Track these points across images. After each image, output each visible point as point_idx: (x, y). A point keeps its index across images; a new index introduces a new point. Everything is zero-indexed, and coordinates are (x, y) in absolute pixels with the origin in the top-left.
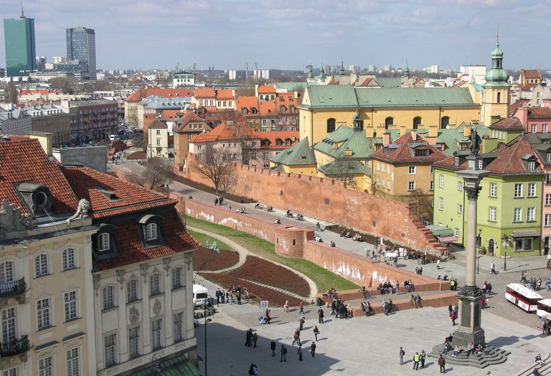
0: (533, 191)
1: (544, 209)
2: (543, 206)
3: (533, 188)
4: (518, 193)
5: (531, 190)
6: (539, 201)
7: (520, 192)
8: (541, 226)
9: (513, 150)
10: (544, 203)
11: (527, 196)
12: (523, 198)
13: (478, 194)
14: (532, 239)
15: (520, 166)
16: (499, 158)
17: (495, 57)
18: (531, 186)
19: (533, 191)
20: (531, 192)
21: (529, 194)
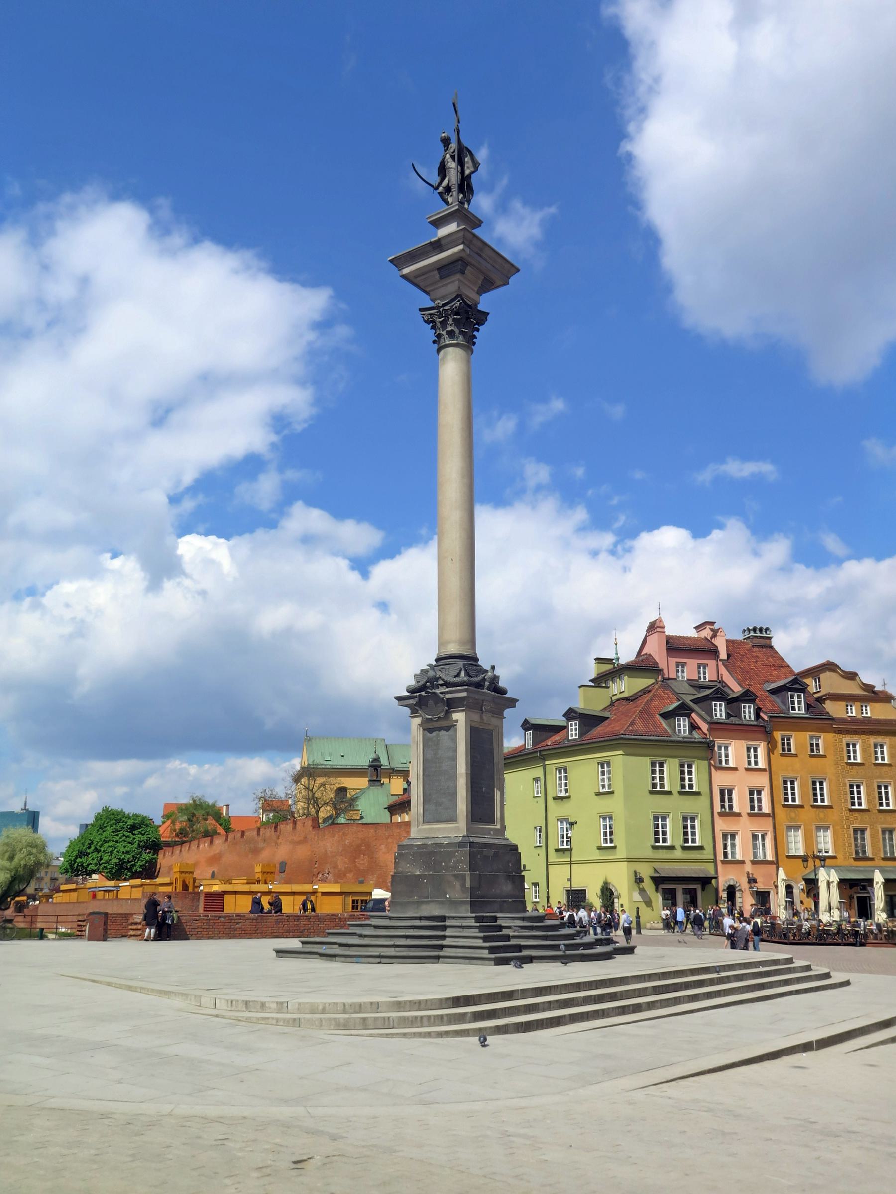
0: (690, 780)
2: (716, 815)
3: (690, 773)
4: (657, 781)
5: (687, 777)
6: (704, 800)
7: (662, 779)
8: (715, 861)
10: (717, 809)
11: (679, 788)
12: (669, 793)
14: (698, 887)
15: (657, 726)
18: (686, 769)
19: (690, 780)
20: (687, 782)
21: (683, 786)
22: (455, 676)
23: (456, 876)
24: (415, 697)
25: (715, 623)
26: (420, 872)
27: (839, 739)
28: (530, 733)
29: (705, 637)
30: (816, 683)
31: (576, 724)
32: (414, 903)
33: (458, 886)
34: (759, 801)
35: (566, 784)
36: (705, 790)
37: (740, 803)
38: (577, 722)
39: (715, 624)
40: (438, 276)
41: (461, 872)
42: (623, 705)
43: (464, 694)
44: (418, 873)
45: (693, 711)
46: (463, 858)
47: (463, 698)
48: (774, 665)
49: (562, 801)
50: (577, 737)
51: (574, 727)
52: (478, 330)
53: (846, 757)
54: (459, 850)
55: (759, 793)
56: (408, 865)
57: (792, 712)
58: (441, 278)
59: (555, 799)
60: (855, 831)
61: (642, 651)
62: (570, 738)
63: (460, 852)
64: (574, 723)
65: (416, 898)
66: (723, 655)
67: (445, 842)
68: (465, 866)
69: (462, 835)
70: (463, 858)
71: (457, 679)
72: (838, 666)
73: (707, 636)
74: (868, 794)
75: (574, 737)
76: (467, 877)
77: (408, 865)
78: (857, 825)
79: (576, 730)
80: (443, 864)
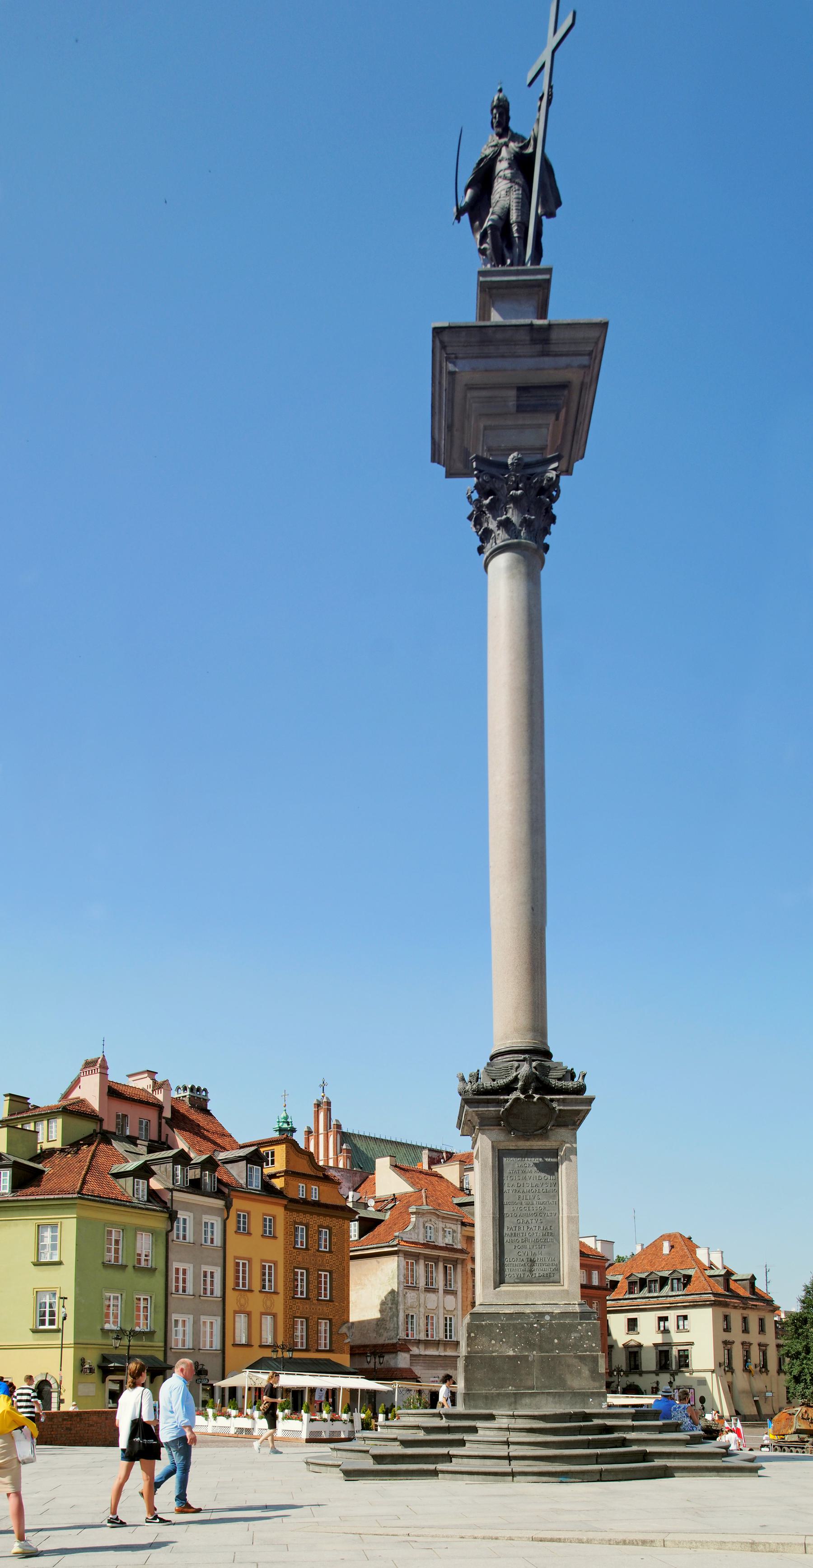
23: (582, 1358)
24: (507, 1101)
26: (514, 1351)
32: (508, 1395)
33: (586, 1372)
41: (588, 1353)
44: (511, 1353)
46: (590, 1334)
54: (583, 1323)
56: (493, 1342)
63: (584, 1325)
65: (510, 1388)
67: (556, 1311)
68: (594, 1345)
69: (577, 1303)
70: (590, 1334)
76: (600, 1360)
77: (493, 1342)
80: (556, 1341)
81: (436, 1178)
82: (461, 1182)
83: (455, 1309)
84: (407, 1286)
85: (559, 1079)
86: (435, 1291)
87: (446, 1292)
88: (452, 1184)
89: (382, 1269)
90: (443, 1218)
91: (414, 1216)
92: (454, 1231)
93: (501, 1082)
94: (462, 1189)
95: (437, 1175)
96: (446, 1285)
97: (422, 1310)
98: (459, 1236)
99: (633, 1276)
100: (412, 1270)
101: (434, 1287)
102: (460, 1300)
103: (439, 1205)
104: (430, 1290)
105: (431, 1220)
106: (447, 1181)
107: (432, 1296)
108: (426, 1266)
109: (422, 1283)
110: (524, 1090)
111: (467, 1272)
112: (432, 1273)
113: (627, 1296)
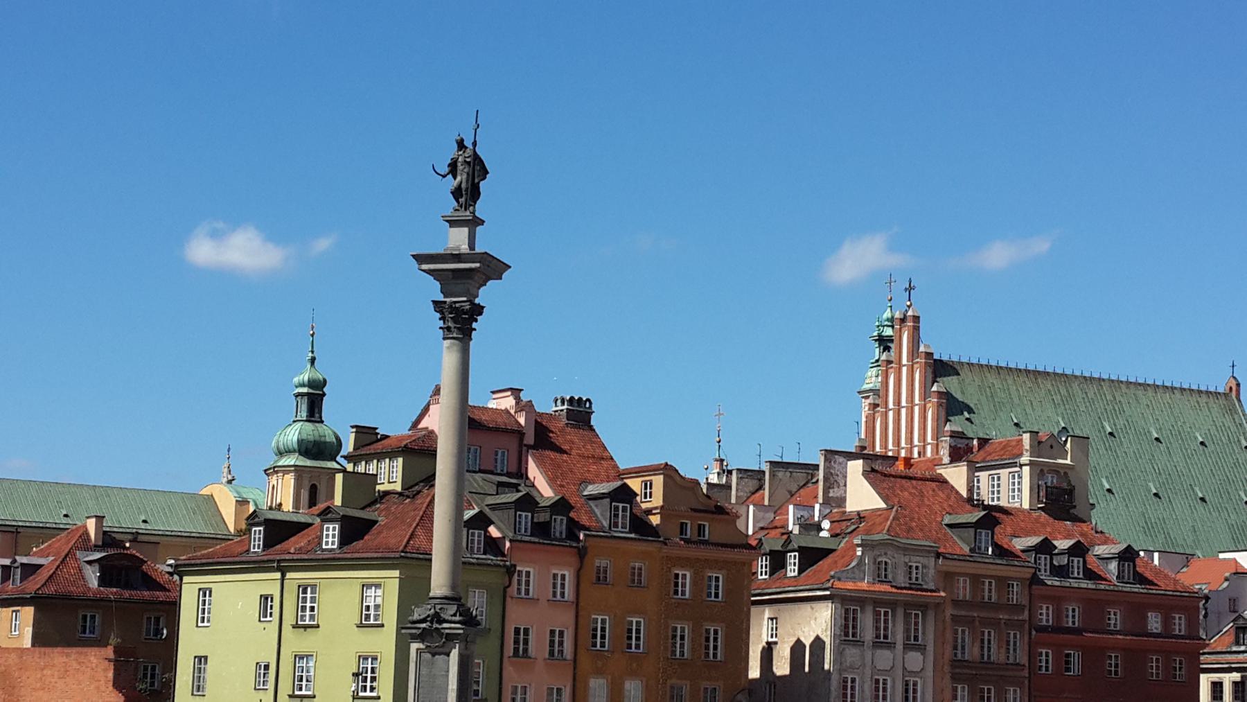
1: (509, 670)
2: (505, 660)
6: (494, 641)
9: (422, 503)
13: (474, 325)
16: (382, 520)
17: (305, 390)
22: (452, 616)
24: (419, 628)
25: (521, 390)
27: (668, 567)
28: (260, 531)
29: (506, 409)
30: (646, 488)
31: (334, 529)
34: (561, 643)
35: (312, 609)
36: (496, 625)
37: (538, 646)
38: (337, 526)
39: (522, 392)
40: (451, 276)
42: (395, 503)
43: (461, 631)
45: (492, 523)
47: (459, 634)
48: (593, 457)
49: (305, 631)
50: (335, 547)
51: (331, 533)
52: (476, 321)
53: (672, 592)
55: (561, 633)
57: (613, 529)
58: (453, 278)
59: (296, 626)
60: (672, 687)
61: (420, 422)
62: (324, 547)
64: (331, 526)
66: (530, 439)
71: (454, 618)
72: (677, 471)
73: (509, 408)
74: (693, 641)
75: (330, 546)
78: (674, 681)
79: (334, 536)
81: (934, 485)
82: (970, 490)
83: (922, 669)
84: (845, 640)
85: (452, 616)
86: (891, 647)
87: (907, 647)
88: (957, 492)
89: (816, 619)
90: (905, 549)
91: (860, 549)
92: (924, 567)
93: (422, 617)
94: (970, 500)
95: (942, 482)
96: (908, 638)
97: (868, 672)
98: (932, 572)
99: (1241, 619)
100: (854, 619)
101: (889, 641)
102: (931, 658)
103: (910, 529)
104: (882, 642)
105: (886, 554)
106: (953, 487)
107: (887, 653)
108: (878, 614)
109: (869, 635)
110: (432, 622)
111: (944, 621)
112: (886, 621)
113: (1234, 649)
